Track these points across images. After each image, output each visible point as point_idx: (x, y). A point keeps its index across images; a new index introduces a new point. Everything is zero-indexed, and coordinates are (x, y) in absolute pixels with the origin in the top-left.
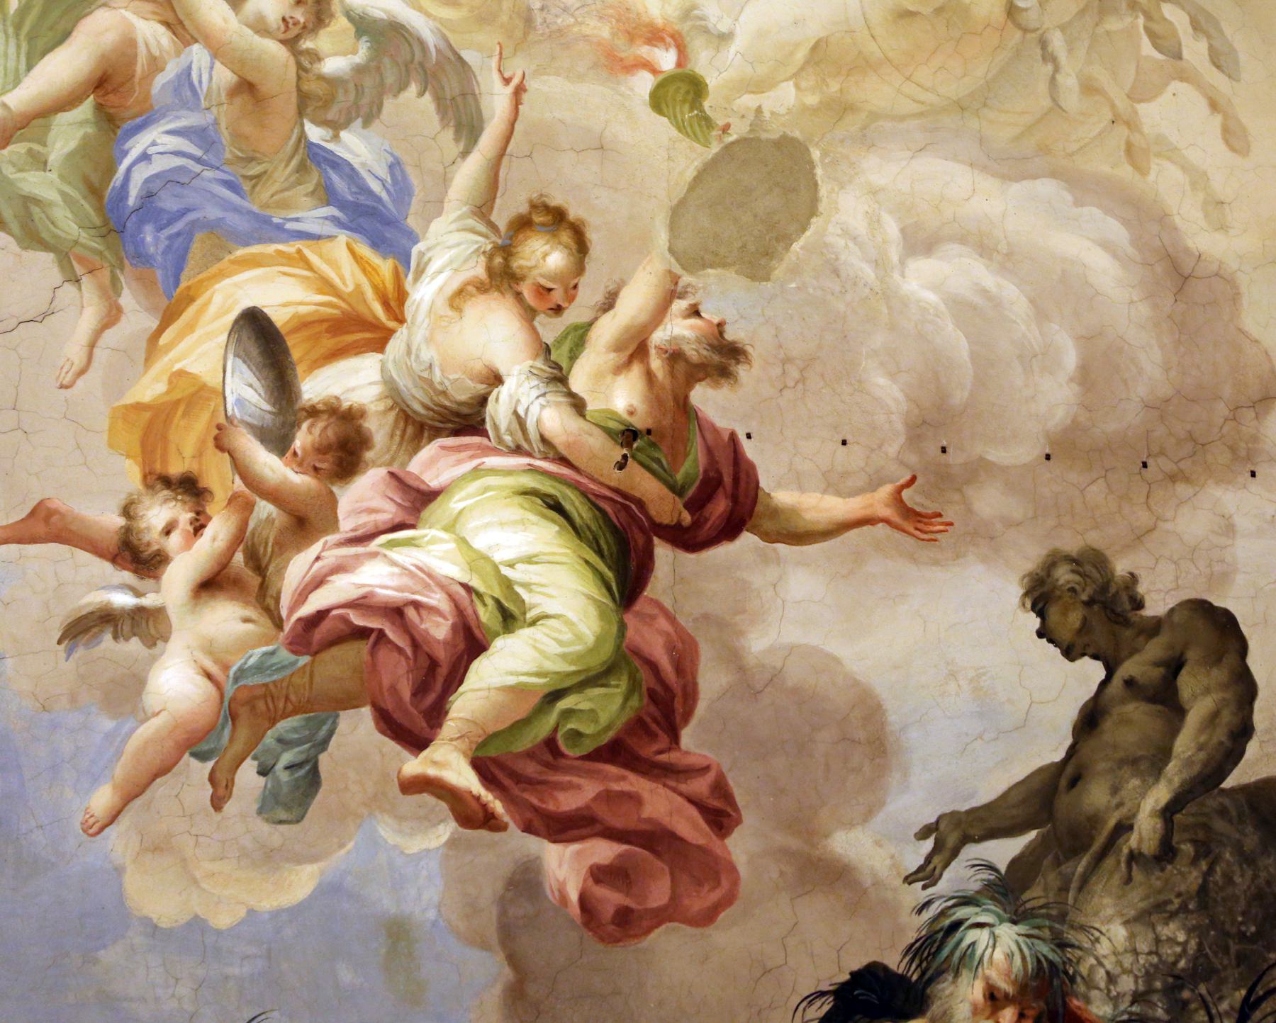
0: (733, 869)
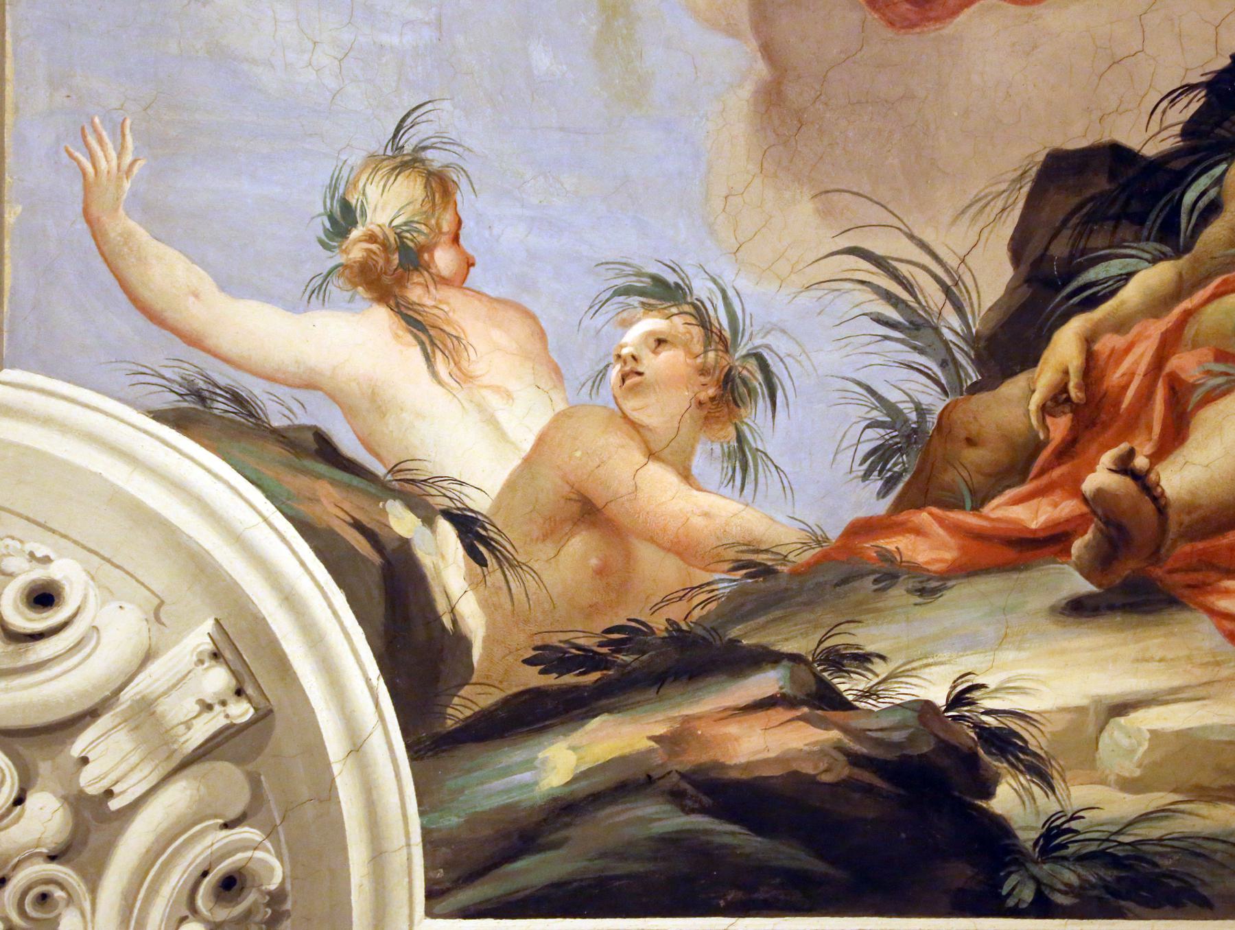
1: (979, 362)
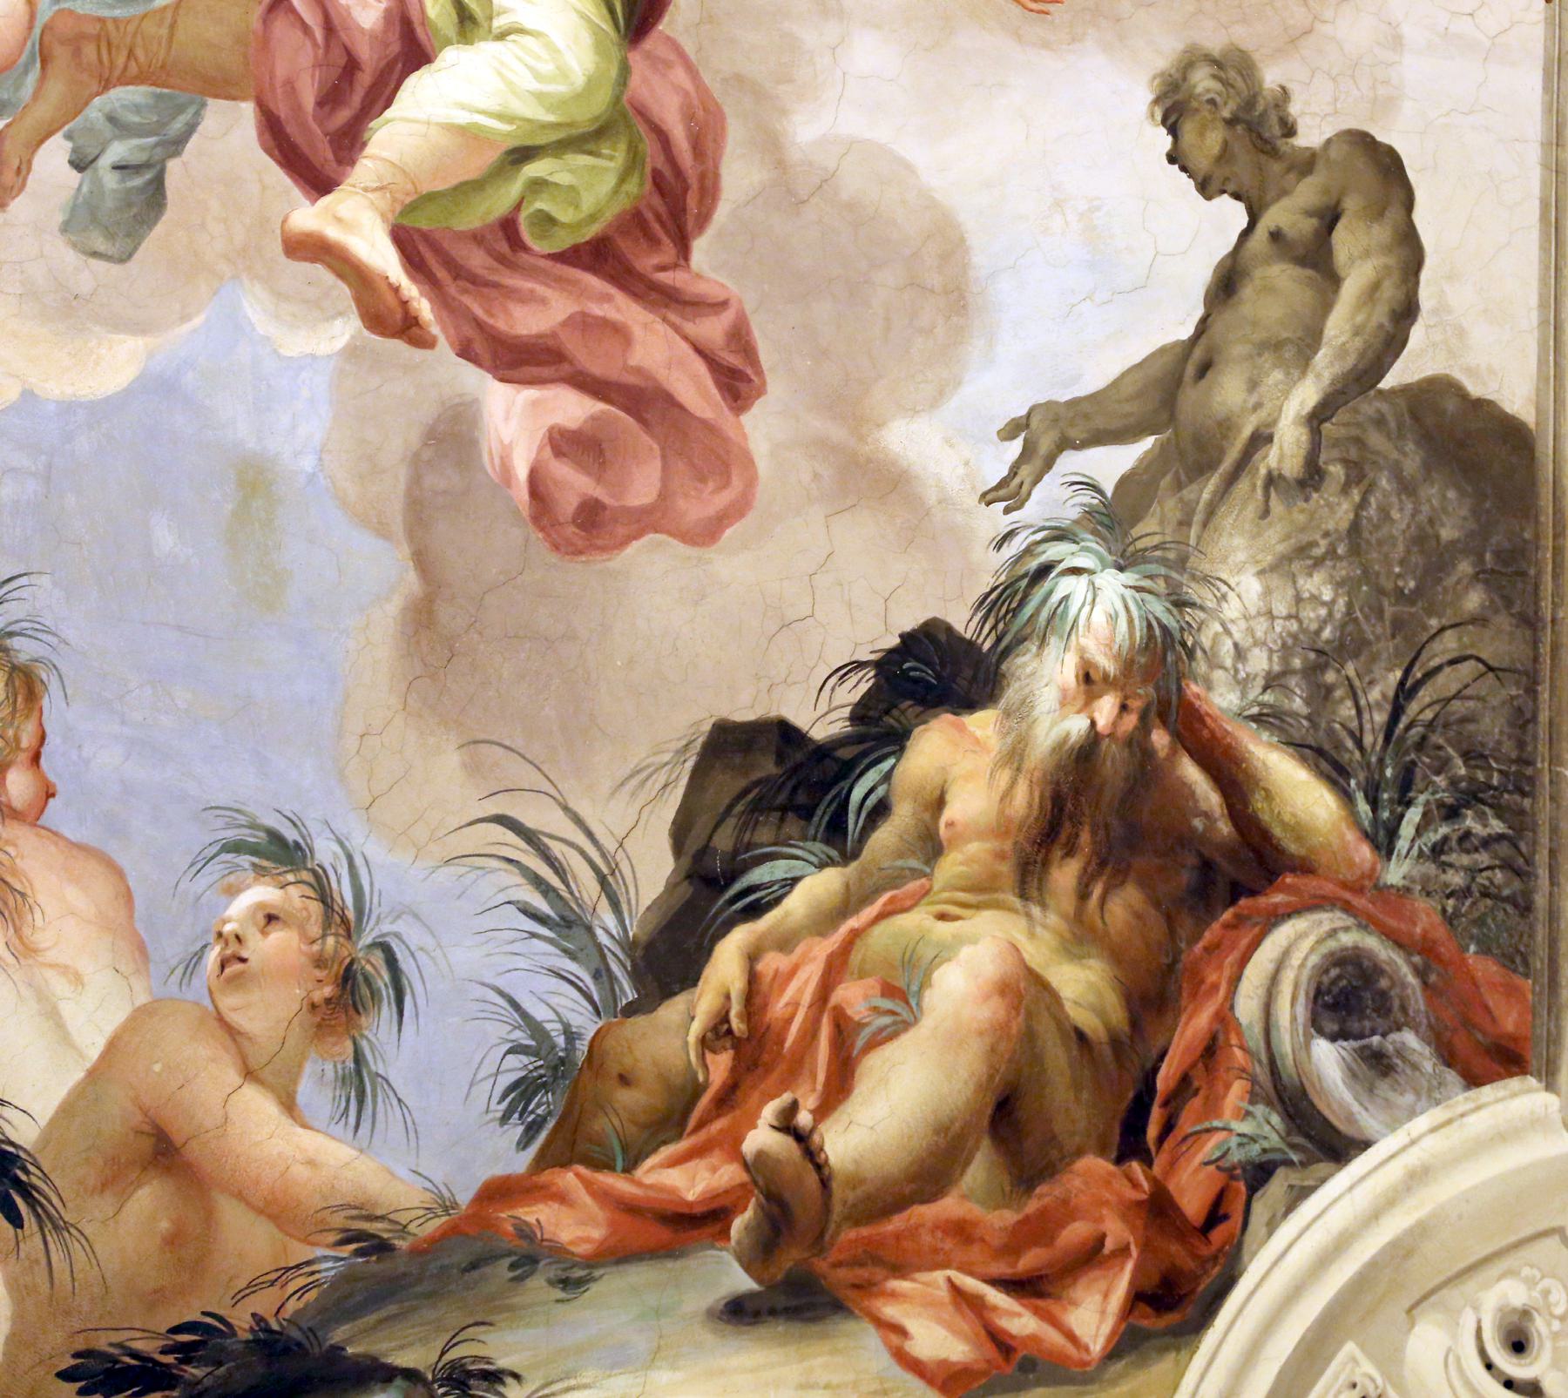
0: (748, 462)
1: (636, 976)
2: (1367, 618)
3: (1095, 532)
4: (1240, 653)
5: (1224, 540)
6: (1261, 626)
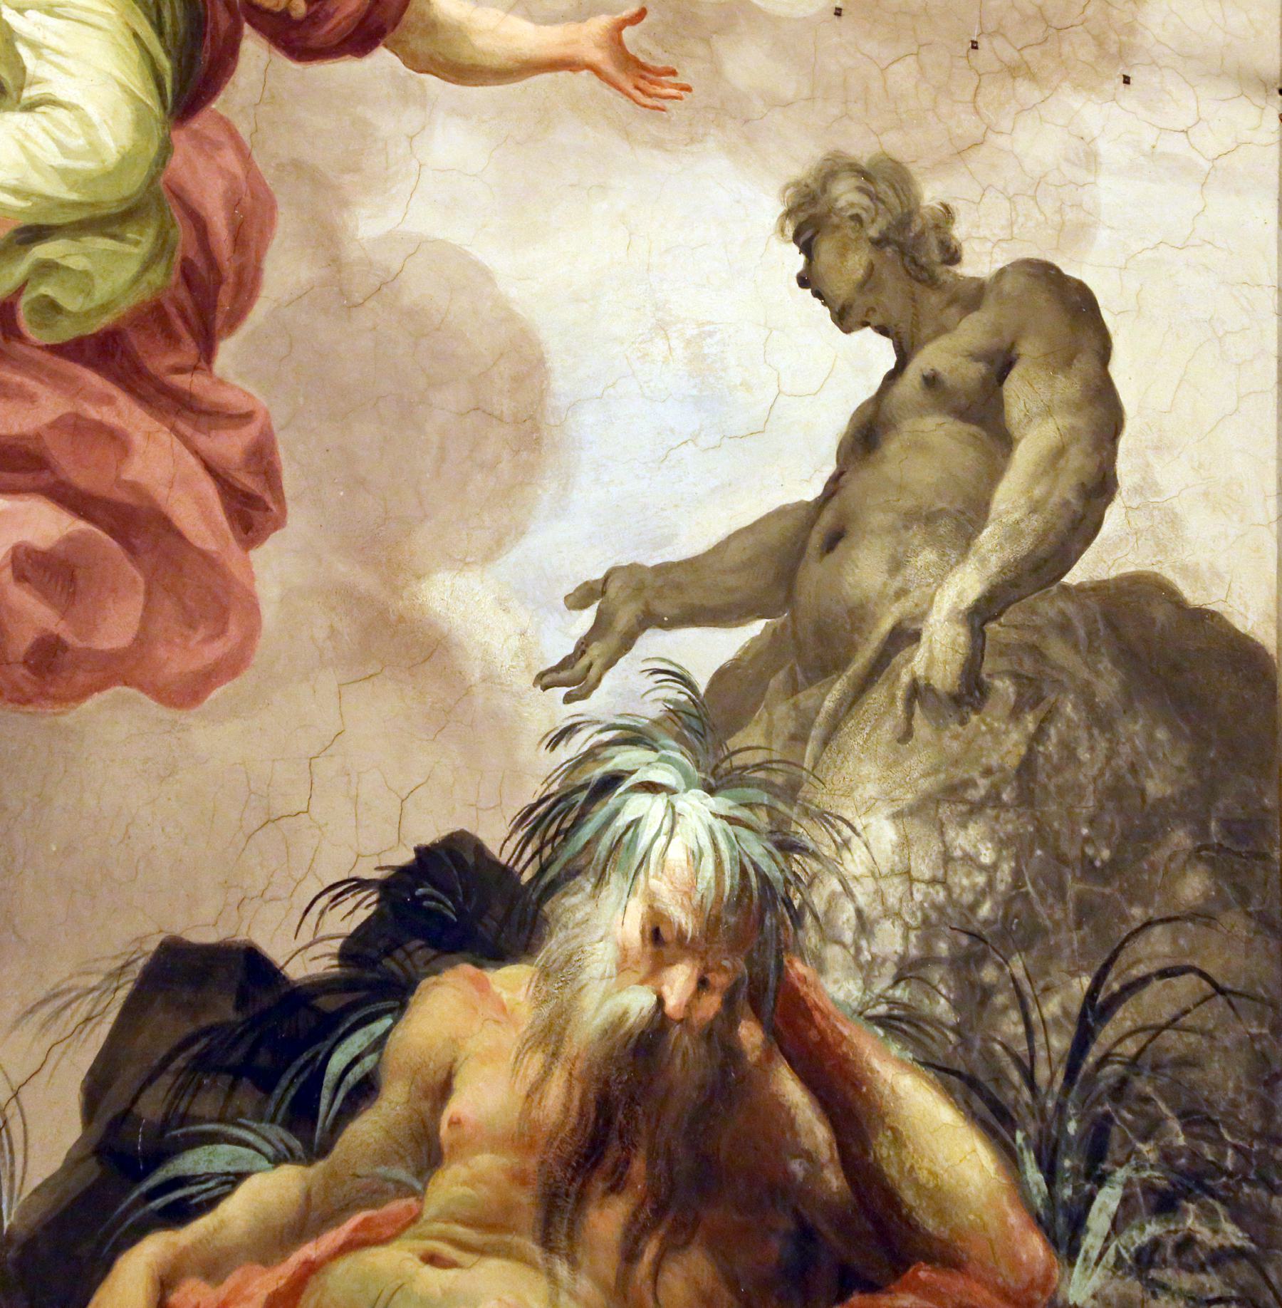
2: (1042, 895)
3: (680, 738)
4: (864, 925)
5: (850, 765)
6: (894, 891)
